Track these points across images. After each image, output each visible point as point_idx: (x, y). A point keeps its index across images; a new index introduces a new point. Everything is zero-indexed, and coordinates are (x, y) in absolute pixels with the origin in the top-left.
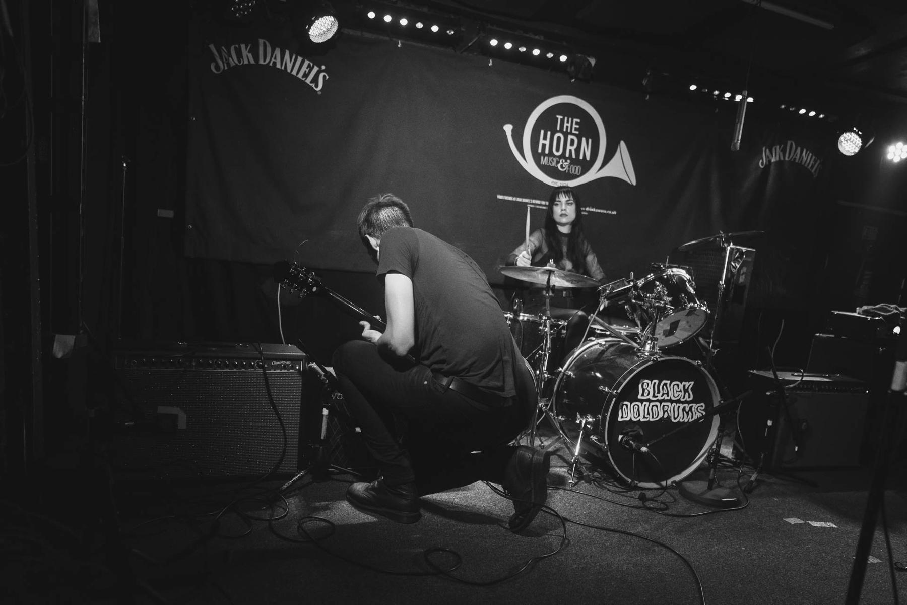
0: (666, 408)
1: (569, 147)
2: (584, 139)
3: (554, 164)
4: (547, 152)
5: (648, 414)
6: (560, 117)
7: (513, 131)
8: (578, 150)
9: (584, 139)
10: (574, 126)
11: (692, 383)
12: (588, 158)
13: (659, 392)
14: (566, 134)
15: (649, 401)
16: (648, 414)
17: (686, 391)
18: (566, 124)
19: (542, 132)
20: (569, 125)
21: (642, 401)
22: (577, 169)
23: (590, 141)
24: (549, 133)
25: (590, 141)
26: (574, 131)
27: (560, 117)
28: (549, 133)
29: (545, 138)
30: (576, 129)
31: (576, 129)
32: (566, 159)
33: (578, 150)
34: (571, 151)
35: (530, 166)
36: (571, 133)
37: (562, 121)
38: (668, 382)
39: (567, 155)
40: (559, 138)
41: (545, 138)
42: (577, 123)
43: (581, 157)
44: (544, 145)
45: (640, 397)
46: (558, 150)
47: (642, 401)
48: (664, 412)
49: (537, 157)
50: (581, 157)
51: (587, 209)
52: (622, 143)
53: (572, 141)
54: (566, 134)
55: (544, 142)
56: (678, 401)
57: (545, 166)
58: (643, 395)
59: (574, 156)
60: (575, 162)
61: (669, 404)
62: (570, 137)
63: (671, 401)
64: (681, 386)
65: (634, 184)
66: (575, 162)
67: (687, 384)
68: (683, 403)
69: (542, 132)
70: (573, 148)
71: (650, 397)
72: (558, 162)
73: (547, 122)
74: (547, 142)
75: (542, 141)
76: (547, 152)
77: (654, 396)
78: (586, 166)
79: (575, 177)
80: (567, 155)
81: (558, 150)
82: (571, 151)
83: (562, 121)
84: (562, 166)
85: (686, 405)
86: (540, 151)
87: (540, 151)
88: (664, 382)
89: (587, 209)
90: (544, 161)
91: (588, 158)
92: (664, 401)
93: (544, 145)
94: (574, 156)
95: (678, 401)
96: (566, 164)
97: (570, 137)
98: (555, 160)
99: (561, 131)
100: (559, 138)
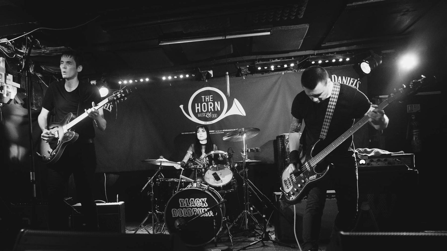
0: (195, 211)
1: (210, 107)
2: (216, 103)
3: (204, 116)
5: (187, 213)
6: (203, 97)
7: (183, 107)
8: (214, 108)
9: (216, 103)
10: (210, 98)
11: (206, 199)
12: (219, 110)
13: (189, 204)
14: (207, 103)
15: (185, 208)
16: (187, 213)
17: (203, 202)
18: (206, 99)
19: (196, 104)
21: (182, 208)
22: (215, 115)
23: (219, 102)
24: (199, 104)
25: (219, 102)
27: (203, 97)
28: (199, 104)
29: (198, 106)
30: (211, 99)
31: (211, 99)
33: (214, 108)
34: (211, 108)
35: (194, 119)
36: (210, 101)
37: (205, 98)
38: (193, 199)
39: (210, 111)
40: (204, 105)
41: (198, 106)
42: (211, 97)
44: (198, 109)
45: (180, 206)
46: (205, 110)
47: (182, 208)
48: (194, 212)
49: (196, 115)
51: (224, 131)
52: (235, 99)
54: (207, 103)
56: (201, 207)
57: (200, 117)
58: (182, 205)
59: (213, 110)
60: (215, 112)
61: (196, 209)
63: (197, 208)
64: (200, 200)
65: (245, 115)
67: (203, 199)
68: (203, 208)
69: (196, 104)
70: (212, 107)
71: (186, 206)
72: (206, 115)
73: (198, 100)
74: (199, 108)
75: (197, 108)
77: (187, 205)
78: (219, 113)
79: (216, 118)
80: (210, 111)
81: (205, 110)
82: (211, 108)
83: (205, 98)
84: (208, 116)
85: (205, 209)
86: (197, 112)
87: (197, 112)
88: (191, 199)
89: (224, 131)
90: (199, 115)
91: (219, 110)
92: (193, 207)
93: (198, 109)
94: (213, 110)
95: (201, 207)
96: (210, 114)
97: (209, 103)
99: (205, 102)
100: (204, 105)
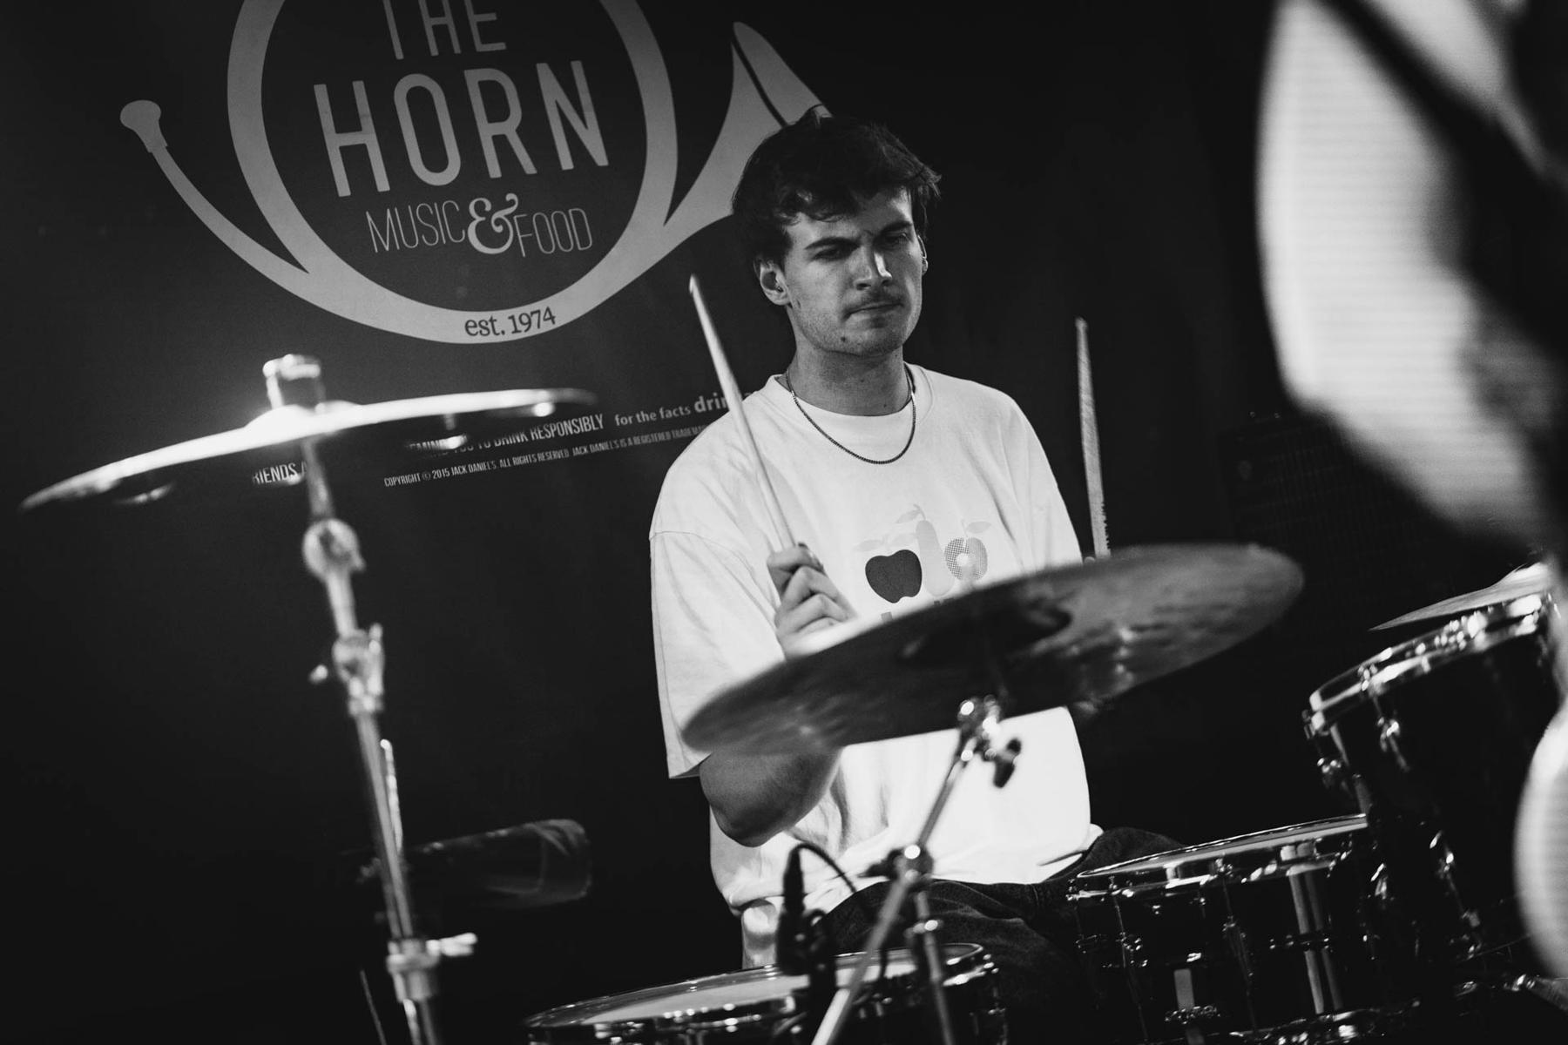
1: (487, 131)
2: (545, 73)
3: (442, 233)
4: (383, 185)
8: (535, 131)
9: (545, 73)
10: (474, 19)
12: (601, 158)
18: (429, 23)
19: (321, 93)
20: (448, 20)
25: (577, 68)
26: (480, 47)
30: (488, 33)
32: (496, 192)
33: (535, 131)
39: (495, 171)
41: (346, 121)
43: (567, 163)
44: (356, 158)
46: (436, 161)
49: (342, 229)
50: (567, 163)
53: (492, 93)
54: (450, 75)
55: (351, 139)
59: (529, 167)
62: (474, 78)
66: (547, 189)
69: (321, 93)
74: (367, 136)
75: (335, 142)
76: (383, 185)
80: (495, 171)
81: (436, 161)
84: (485, 233)
86: (344, 189)
87: (344, 189)
91: (601, 158)
94: (529, 167)
97: (474, 78)
98: (439, 211)
99: (418, 61)
